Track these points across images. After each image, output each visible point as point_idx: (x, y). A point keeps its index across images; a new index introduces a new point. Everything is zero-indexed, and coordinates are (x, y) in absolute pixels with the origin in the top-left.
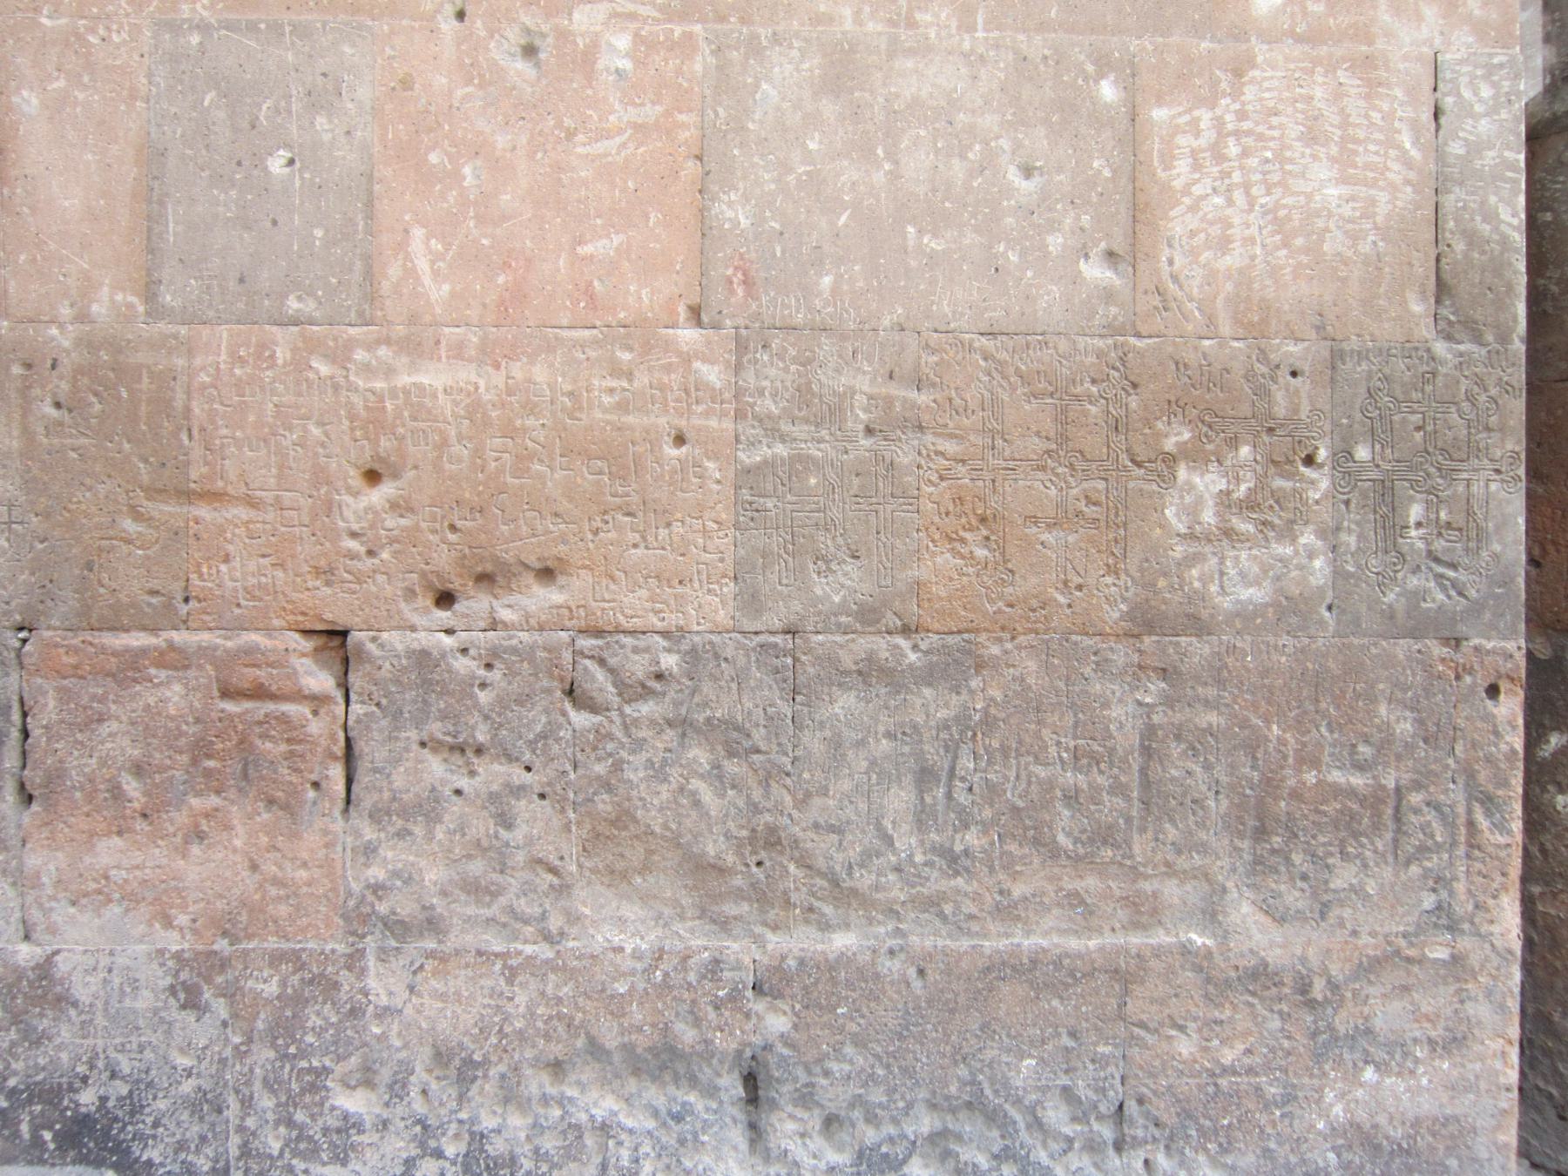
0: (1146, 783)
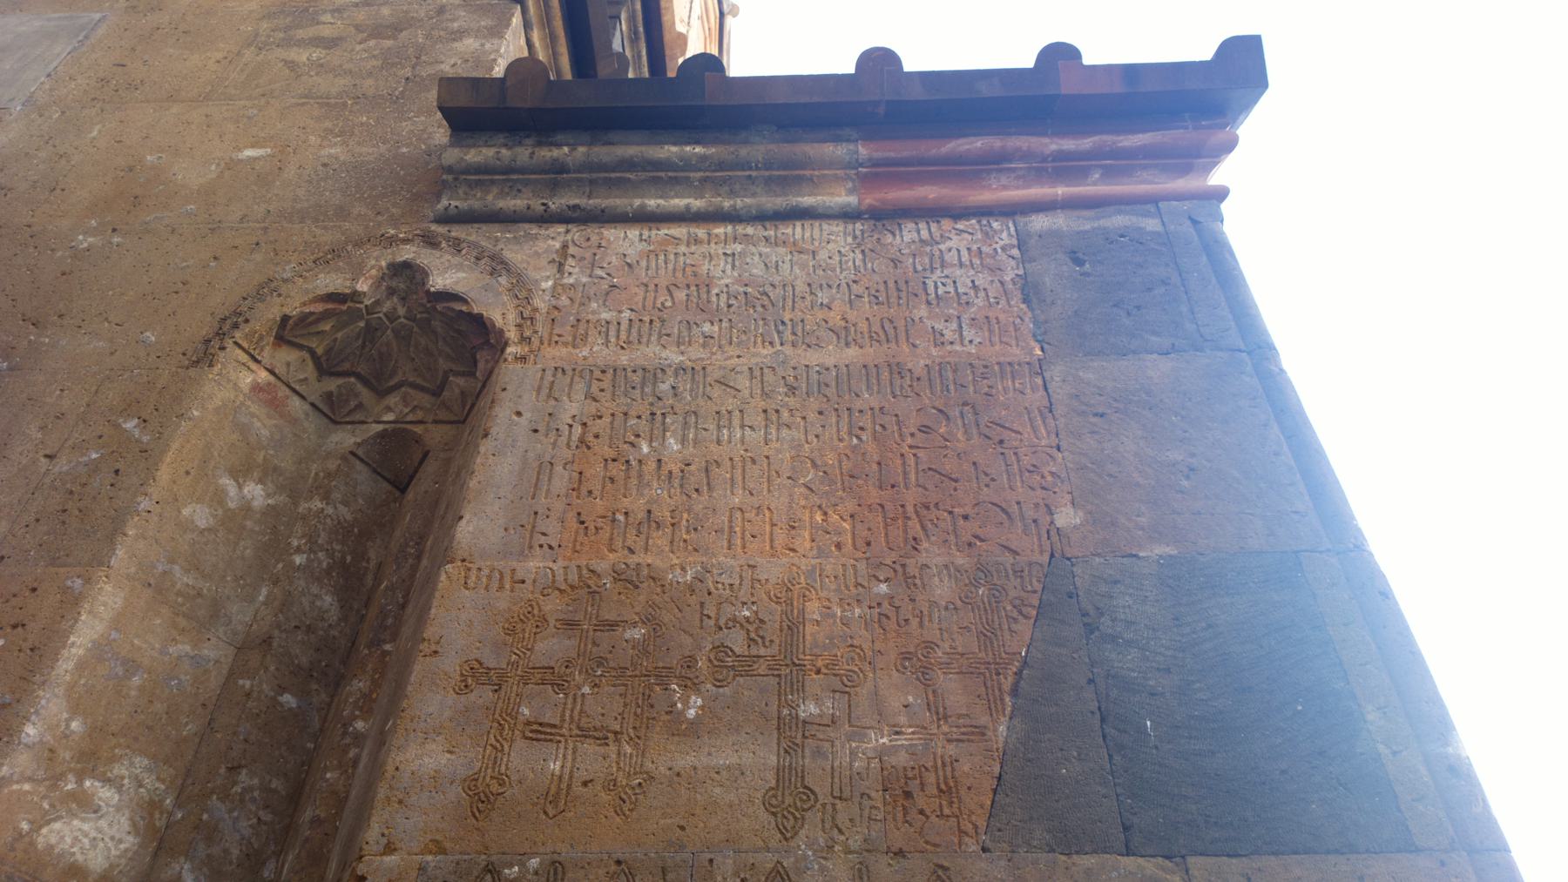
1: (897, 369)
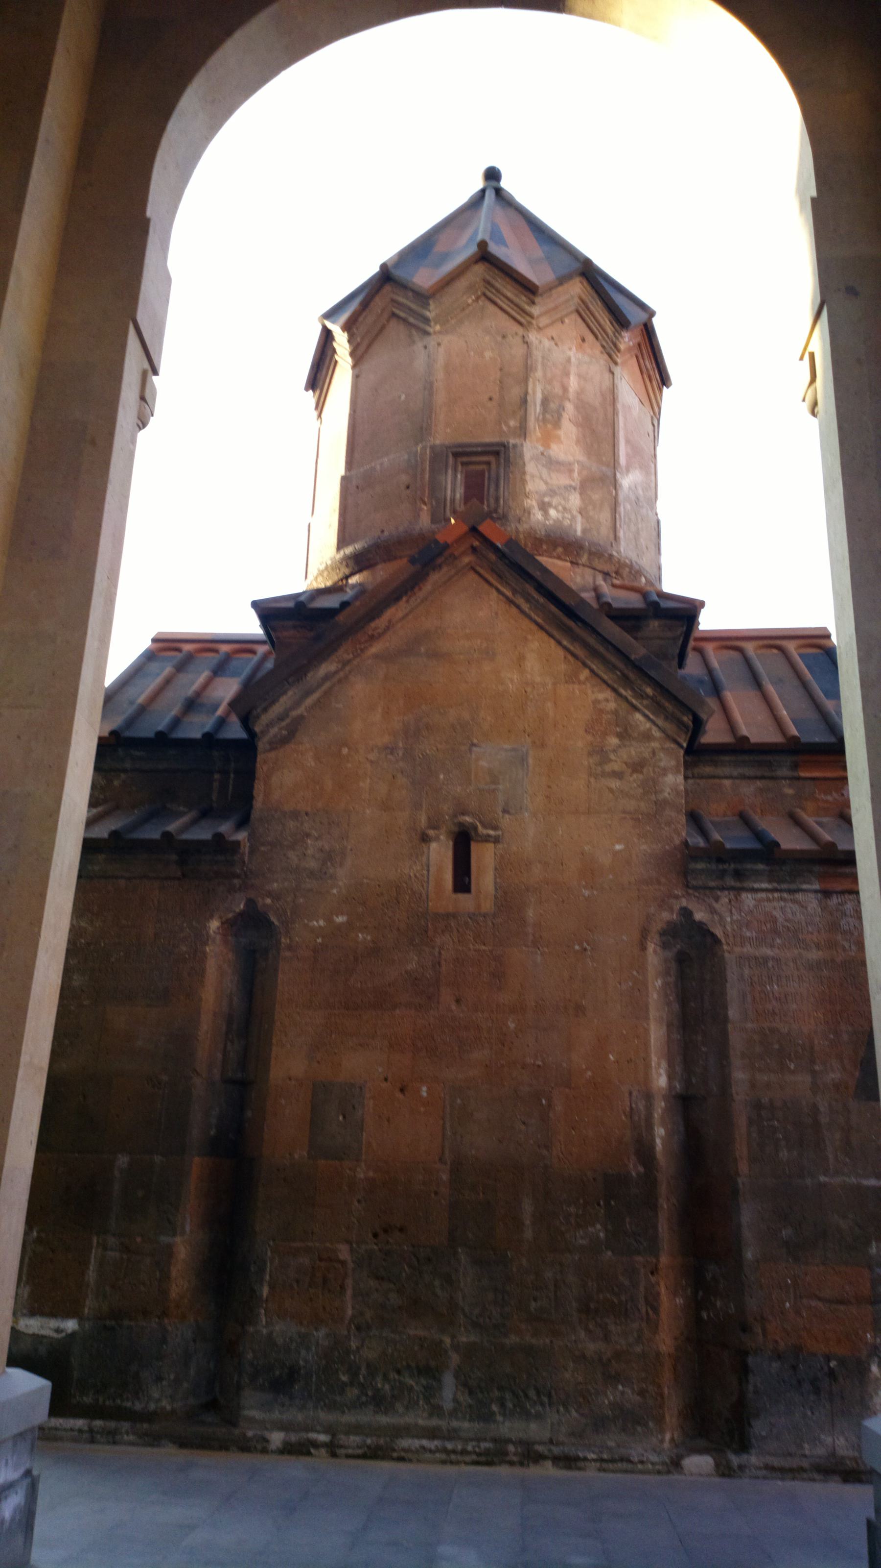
1: (833, 961)
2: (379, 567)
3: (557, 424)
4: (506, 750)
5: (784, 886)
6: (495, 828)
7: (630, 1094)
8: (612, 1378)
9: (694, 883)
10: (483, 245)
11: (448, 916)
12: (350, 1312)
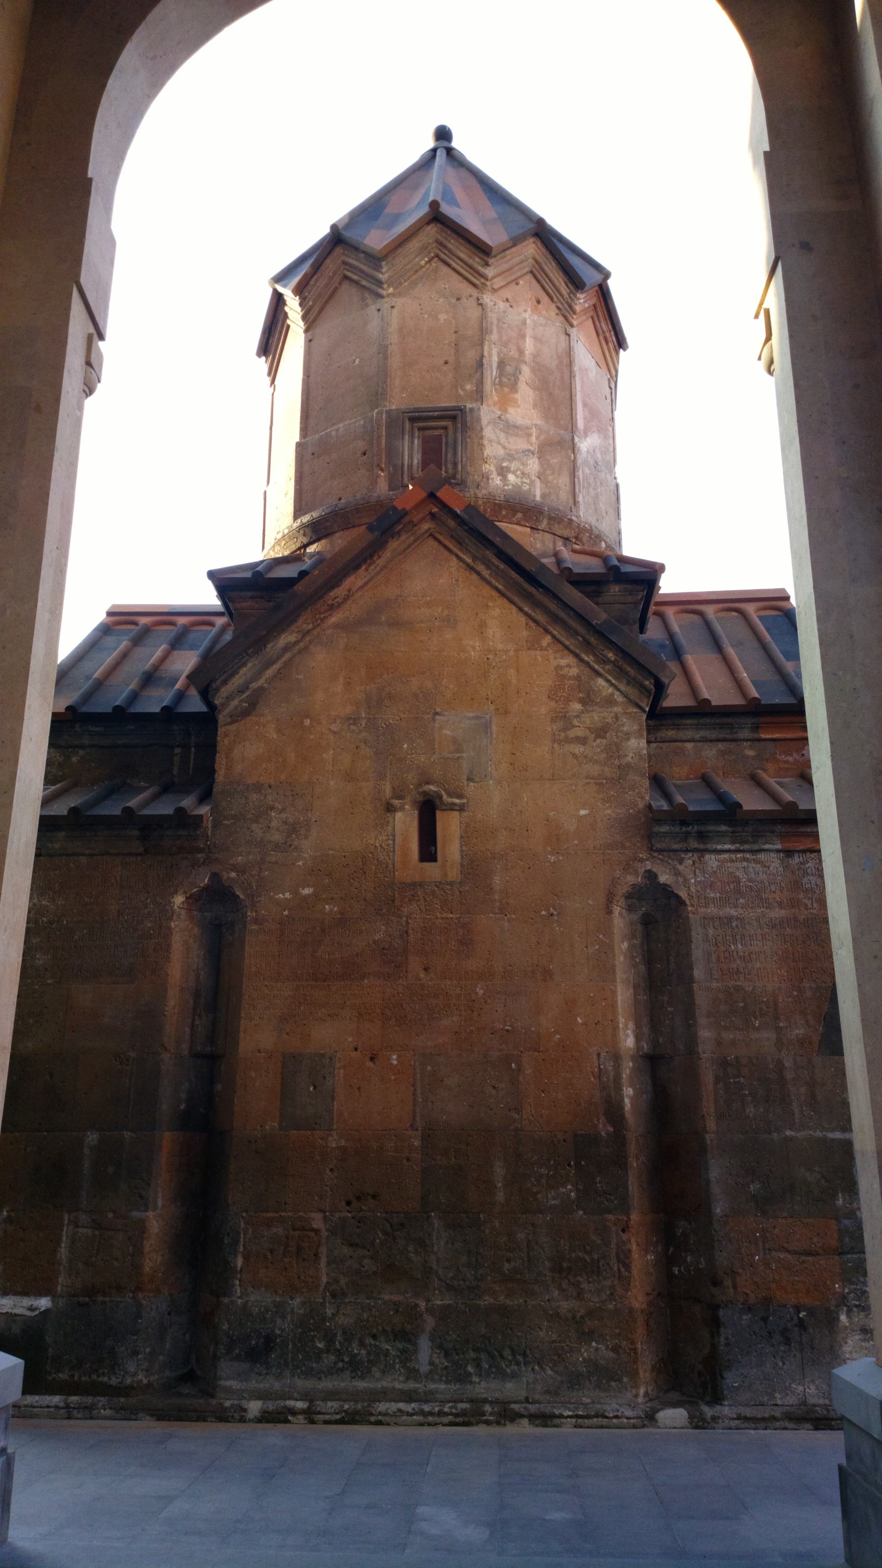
0: (528, 1254)
1: (796, 919)
2: (338, 535)
3: (514, 388)
4: (470, 718)
5: (746, 847)
6: (460, 797)
7: (599, 1055)
8: (587, 1336)
9: (658, 846)
10: (434, 205)
11: (414, 885)
12: (324, 1280)
